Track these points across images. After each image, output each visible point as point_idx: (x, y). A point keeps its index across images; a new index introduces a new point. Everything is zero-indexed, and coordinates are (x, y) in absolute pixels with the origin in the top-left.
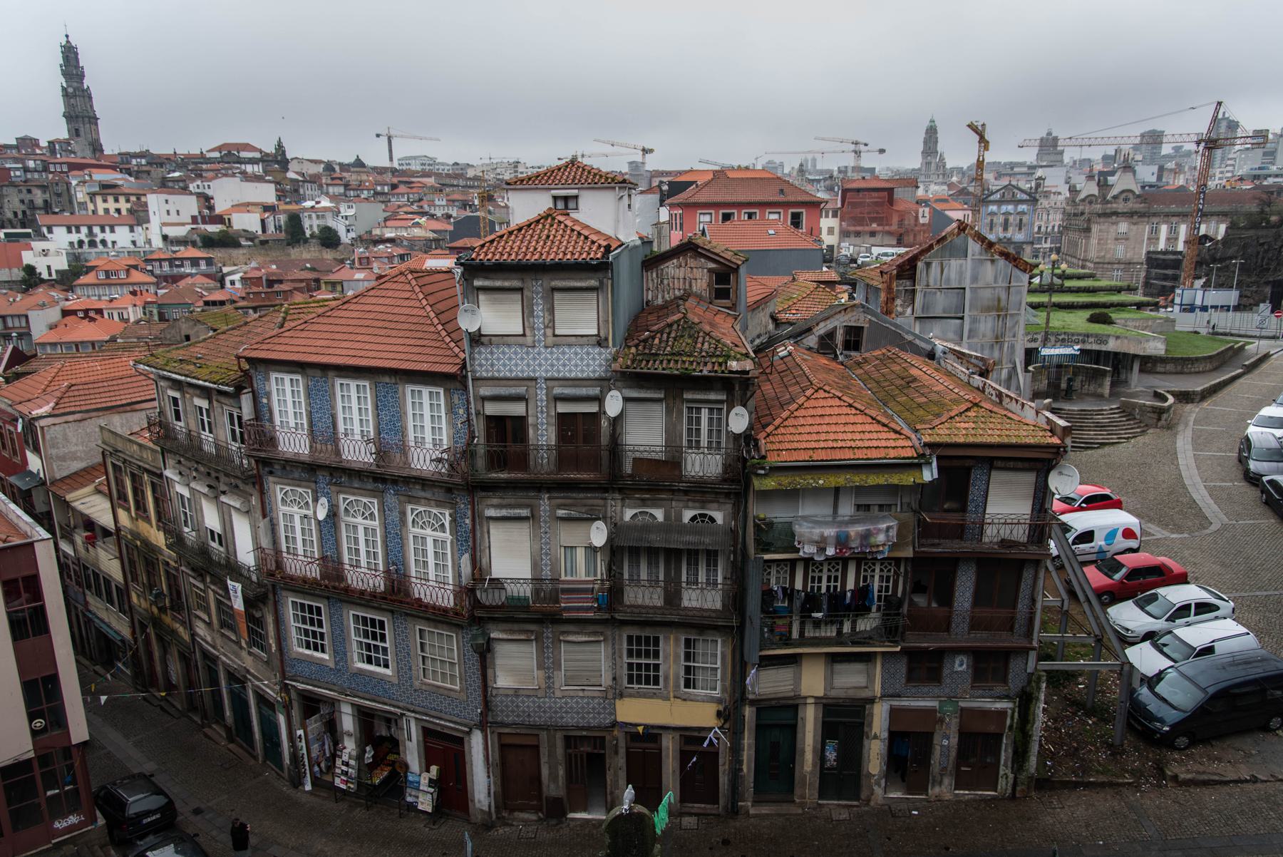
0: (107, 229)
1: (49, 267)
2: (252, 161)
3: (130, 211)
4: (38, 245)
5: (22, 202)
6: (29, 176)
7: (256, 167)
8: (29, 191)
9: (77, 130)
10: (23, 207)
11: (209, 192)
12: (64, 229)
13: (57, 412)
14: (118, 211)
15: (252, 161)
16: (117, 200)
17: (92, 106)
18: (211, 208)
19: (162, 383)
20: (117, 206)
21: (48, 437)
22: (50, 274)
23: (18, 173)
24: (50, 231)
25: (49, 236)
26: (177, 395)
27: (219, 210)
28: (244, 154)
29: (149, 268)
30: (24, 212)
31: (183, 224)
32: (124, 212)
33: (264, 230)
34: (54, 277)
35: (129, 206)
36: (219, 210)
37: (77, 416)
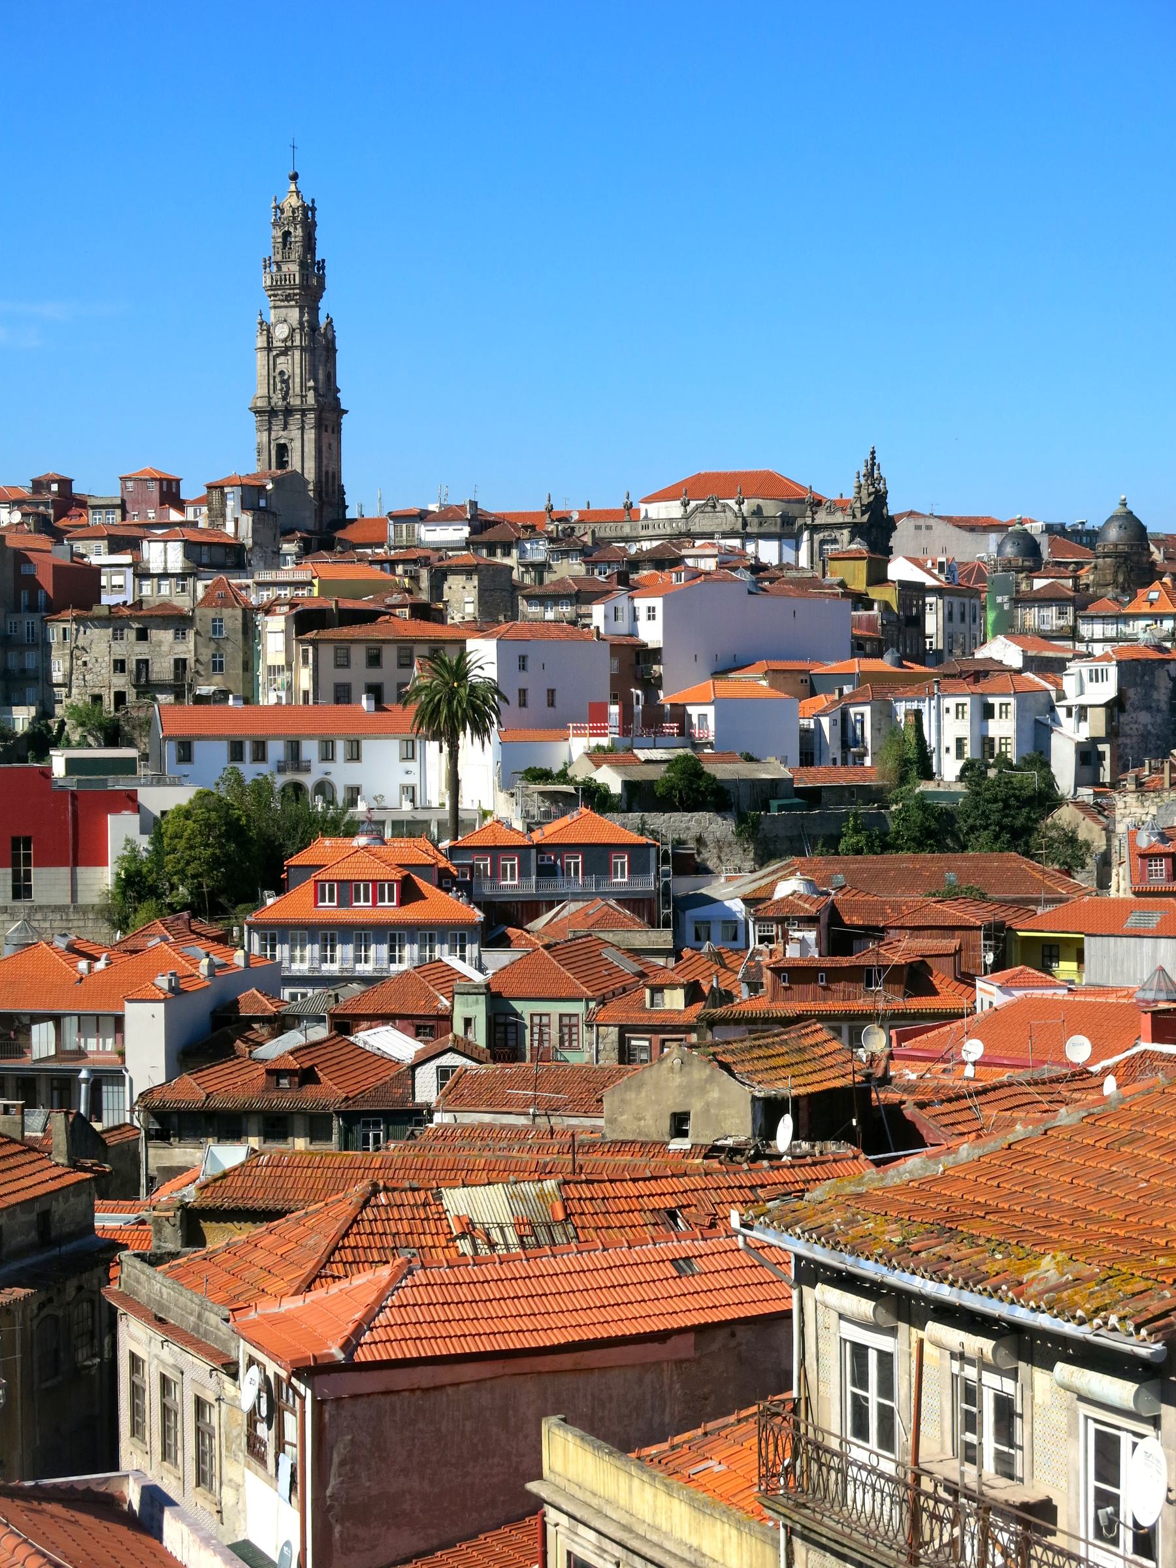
0: (340, 747)
6: (147, 588)
8: (142, 635)
9: (282, 450)
10: (121, 682)
11: (651, 633)
12: (223, 748)
16: (374, 660)
17: (331, 377)
20: (374, 676)
23: (118, 580)
24: (185, 753)
25: (185, 768)
30: (120, 697)
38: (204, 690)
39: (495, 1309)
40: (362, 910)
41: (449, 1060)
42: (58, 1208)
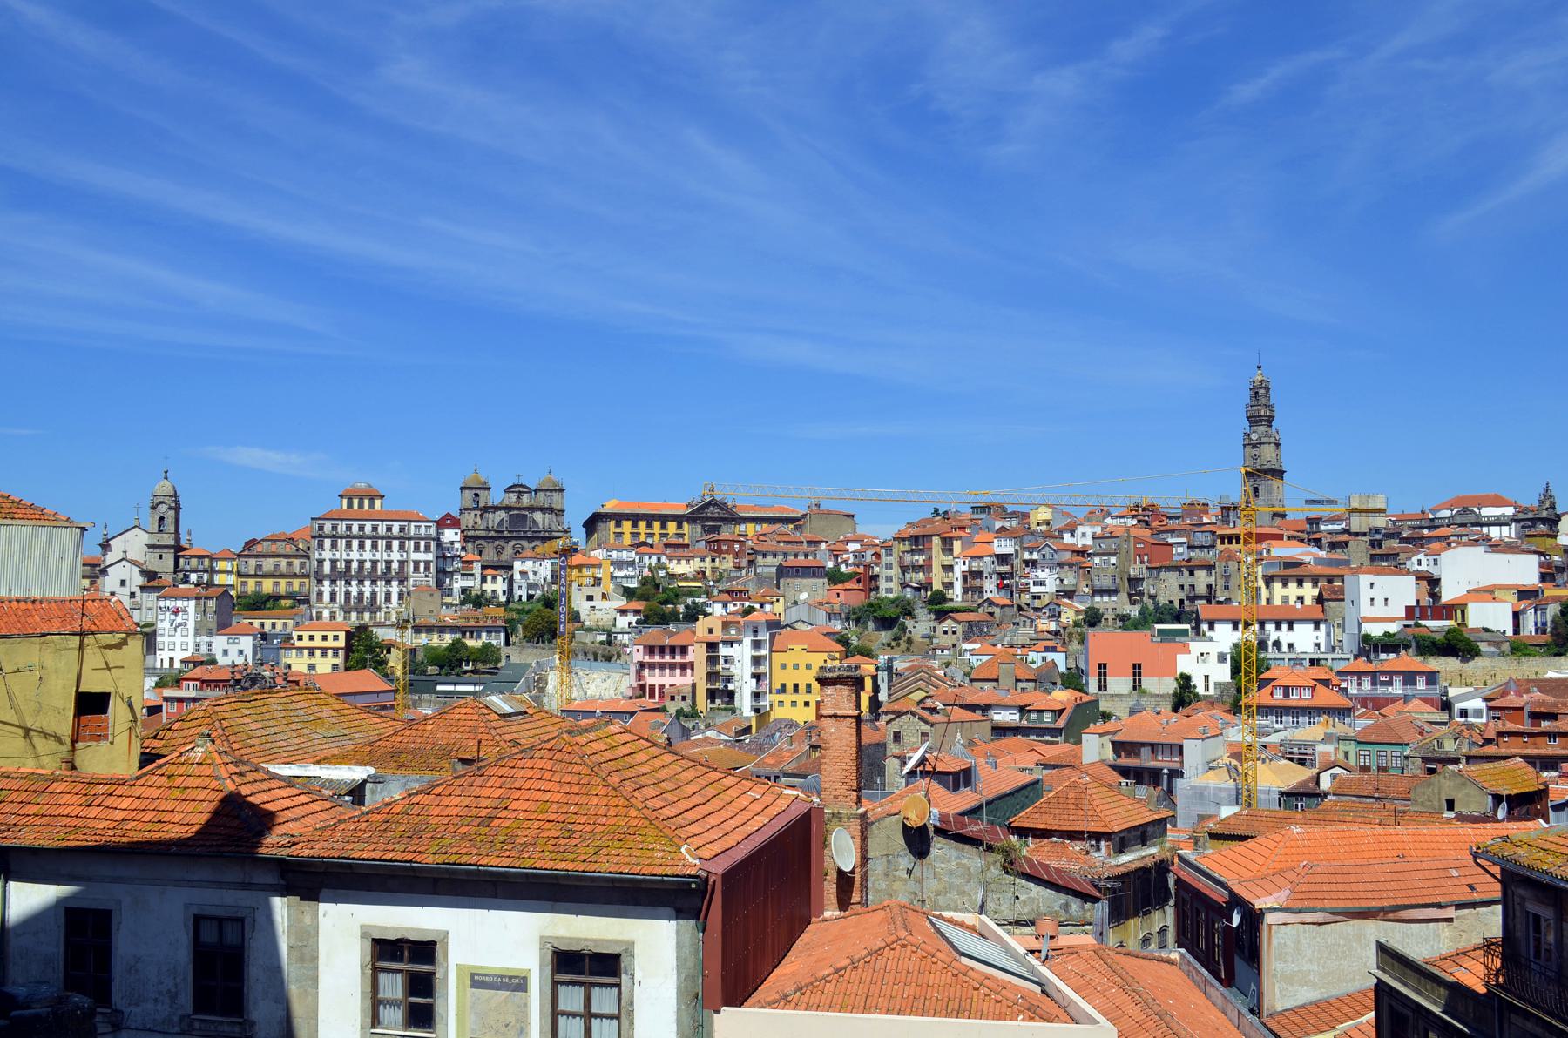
0: (1284, 627)
1: (1207, 677)
2: (1499, 522)
3: (1320, 600)
4: (1196, 647)
5: (1182, 587)
7: (1505, 529)
8: (1192, 574)
9: (1256, 490)
10: (1182, 595)
13: (1291, 905)
14: (1301, 599)
15: (1499, 522)
18: (1435, 596)
19: (1521, 891)
20: (1300, 592)
21: (1275, 942)
22: (1207, 688)
24: (1211, 628)
26: (1546, 913)
27: (1448, 594)
28: (1486, 511)
29: (1344, 685)
30: (1182, 602)
31: (1392, 620)
32: (1308, 601)
33: (1516, 630)
34: (1212, 692)
35: (1316, 592)
36: (1448, 594)
37: (1319, 917)
38: (1222, 599)
39: (1354, 887)
40: (1294, 699)
41: (1337, 770)
42: (1150, 829)
